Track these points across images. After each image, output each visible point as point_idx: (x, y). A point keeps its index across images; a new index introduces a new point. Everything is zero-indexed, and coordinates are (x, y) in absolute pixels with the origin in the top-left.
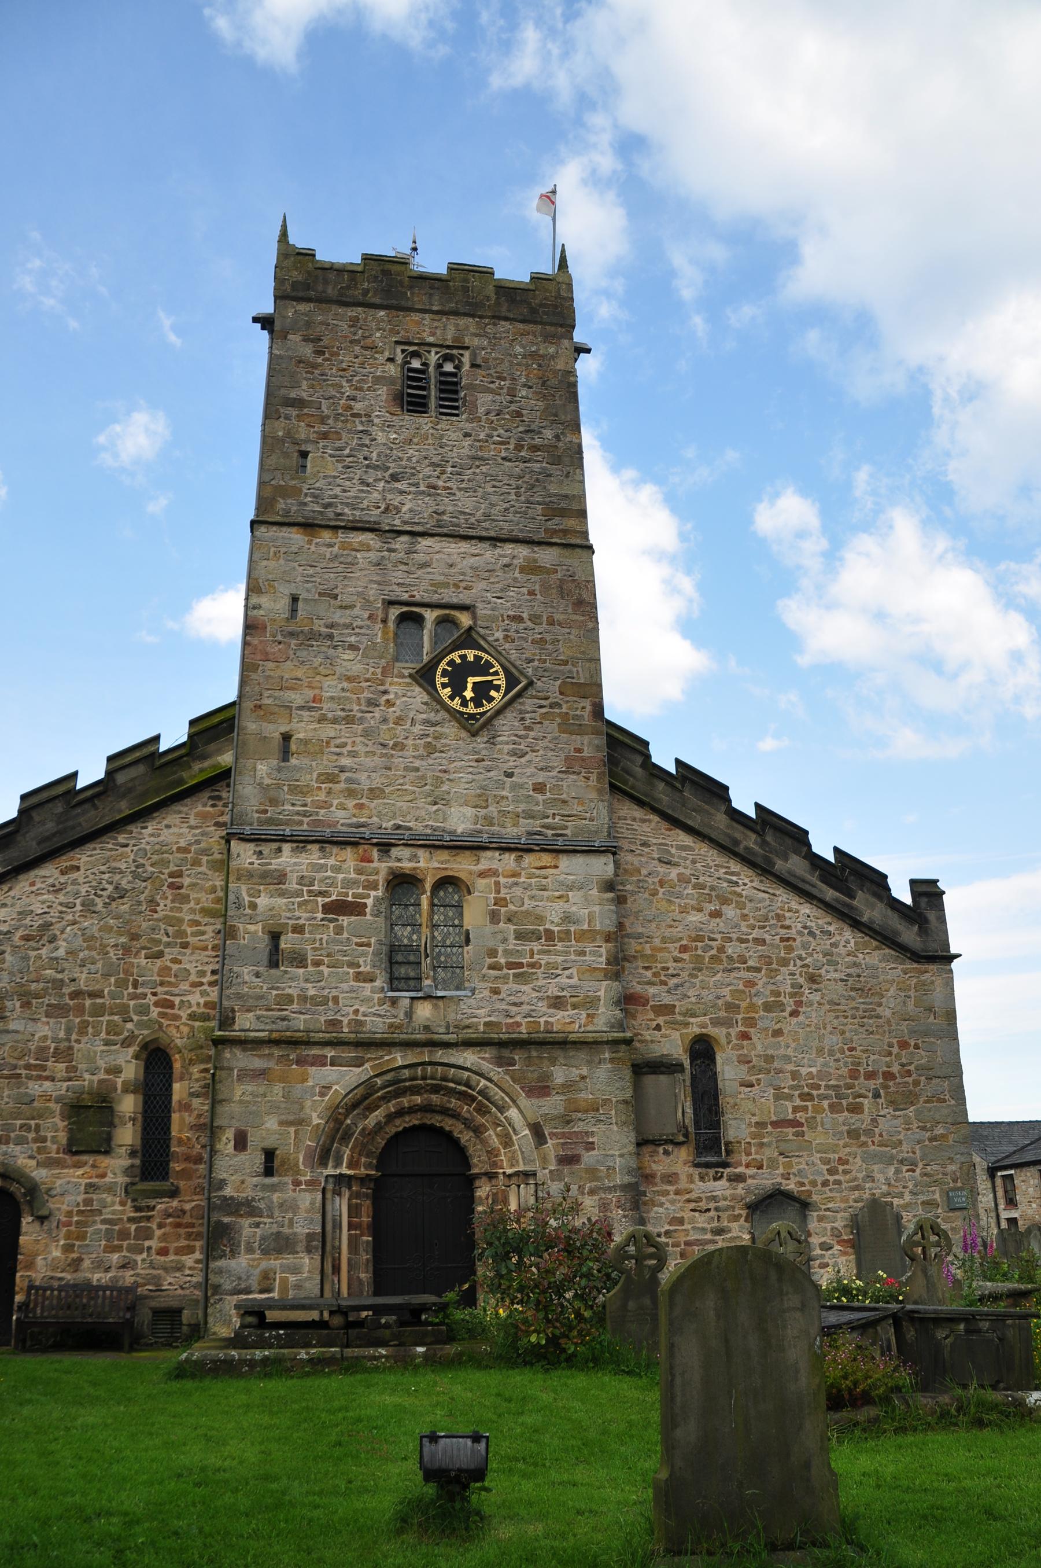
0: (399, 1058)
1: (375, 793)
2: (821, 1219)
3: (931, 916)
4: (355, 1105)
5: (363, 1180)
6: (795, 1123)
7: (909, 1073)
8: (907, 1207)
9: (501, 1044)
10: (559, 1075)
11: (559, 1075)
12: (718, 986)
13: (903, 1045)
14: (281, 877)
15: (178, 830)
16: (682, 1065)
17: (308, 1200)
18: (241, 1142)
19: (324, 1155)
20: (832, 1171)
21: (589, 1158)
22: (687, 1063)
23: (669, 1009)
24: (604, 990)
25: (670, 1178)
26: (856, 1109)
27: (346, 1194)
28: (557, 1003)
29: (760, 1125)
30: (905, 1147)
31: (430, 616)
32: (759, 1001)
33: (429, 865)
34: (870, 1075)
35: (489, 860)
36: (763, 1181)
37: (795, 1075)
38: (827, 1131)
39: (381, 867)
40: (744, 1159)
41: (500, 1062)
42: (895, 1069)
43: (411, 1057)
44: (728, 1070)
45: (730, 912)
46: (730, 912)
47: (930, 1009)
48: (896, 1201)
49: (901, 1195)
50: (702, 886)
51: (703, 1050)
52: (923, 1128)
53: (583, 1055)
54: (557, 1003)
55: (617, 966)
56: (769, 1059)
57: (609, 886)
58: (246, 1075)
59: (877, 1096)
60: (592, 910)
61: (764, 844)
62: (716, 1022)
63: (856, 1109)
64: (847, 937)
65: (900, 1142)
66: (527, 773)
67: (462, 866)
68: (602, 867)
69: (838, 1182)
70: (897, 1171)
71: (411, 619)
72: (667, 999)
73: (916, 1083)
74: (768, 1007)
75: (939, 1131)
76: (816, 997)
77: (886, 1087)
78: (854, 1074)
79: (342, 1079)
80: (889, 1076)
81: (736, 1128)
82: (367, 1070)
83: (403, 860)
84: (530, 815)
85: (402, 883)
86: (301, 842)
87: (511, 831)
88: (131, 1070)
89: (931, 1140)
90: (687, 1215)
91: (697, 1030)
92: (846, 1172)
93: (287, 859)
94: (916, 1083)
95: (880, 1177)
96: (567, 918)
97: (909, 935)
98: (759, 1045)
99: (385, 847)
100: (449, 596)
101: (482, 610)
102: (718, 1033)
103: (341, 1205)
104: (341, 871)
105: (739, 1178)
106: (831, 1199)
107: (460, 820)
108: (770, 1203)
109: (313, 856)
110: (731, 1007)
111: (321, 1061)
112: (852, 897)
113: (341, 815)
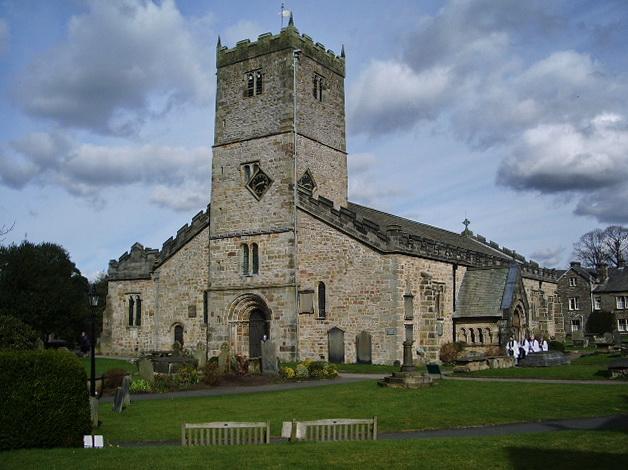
0: (242, 292)
9: (263, 288)
11: (276, 295)
12: (324, 267)
13: (378, 282)
14: (218, 248)
15: (204, 236)
16: (313, 292)
17: (224, 328)
18: (212, 315)
22: (317, 291)
23: (311, 274)
24: (287, 271)
28: (277, 276)
33: (249, 240)
35: (264, 237)
38: (353, 308)
39: (239, 242)
41: (263, 293)
43: (246, 292)
44: (328, 292)
46: (329, 243)
51: (322, 286)
53: (281, 290)
54: (277, 276)
55: (291, 265)
56: (337, 288)
57: (292, 241)
58: (214, 298)
60: (285, 248)
61: (340, 220)
62: (324, 278)
63: (361, 303)
64: (362, 248)
66: (273, 210)
67: (257, 239)
68: (290, 235)
71: (247, 168)
78: (362, 292)
80: (373, 292)
81: (328, 309)
82: (235, 296)
83: (244, 240)
84: (273, 222)
86: (223, 238)
87: (268, 228)
88: (201, 297)
93: (221, 243)
96: (280, 251)
97: (383, 246)
98: (336, 283)
100: (255, 158)
101: (263, 161)
103: (234, 329)
104: (230, 245)
107: (256, 227)
108: (334, 330)
109: (225, 241)
110: (329, 273)
111: (227, 294)
113: (232, 230)
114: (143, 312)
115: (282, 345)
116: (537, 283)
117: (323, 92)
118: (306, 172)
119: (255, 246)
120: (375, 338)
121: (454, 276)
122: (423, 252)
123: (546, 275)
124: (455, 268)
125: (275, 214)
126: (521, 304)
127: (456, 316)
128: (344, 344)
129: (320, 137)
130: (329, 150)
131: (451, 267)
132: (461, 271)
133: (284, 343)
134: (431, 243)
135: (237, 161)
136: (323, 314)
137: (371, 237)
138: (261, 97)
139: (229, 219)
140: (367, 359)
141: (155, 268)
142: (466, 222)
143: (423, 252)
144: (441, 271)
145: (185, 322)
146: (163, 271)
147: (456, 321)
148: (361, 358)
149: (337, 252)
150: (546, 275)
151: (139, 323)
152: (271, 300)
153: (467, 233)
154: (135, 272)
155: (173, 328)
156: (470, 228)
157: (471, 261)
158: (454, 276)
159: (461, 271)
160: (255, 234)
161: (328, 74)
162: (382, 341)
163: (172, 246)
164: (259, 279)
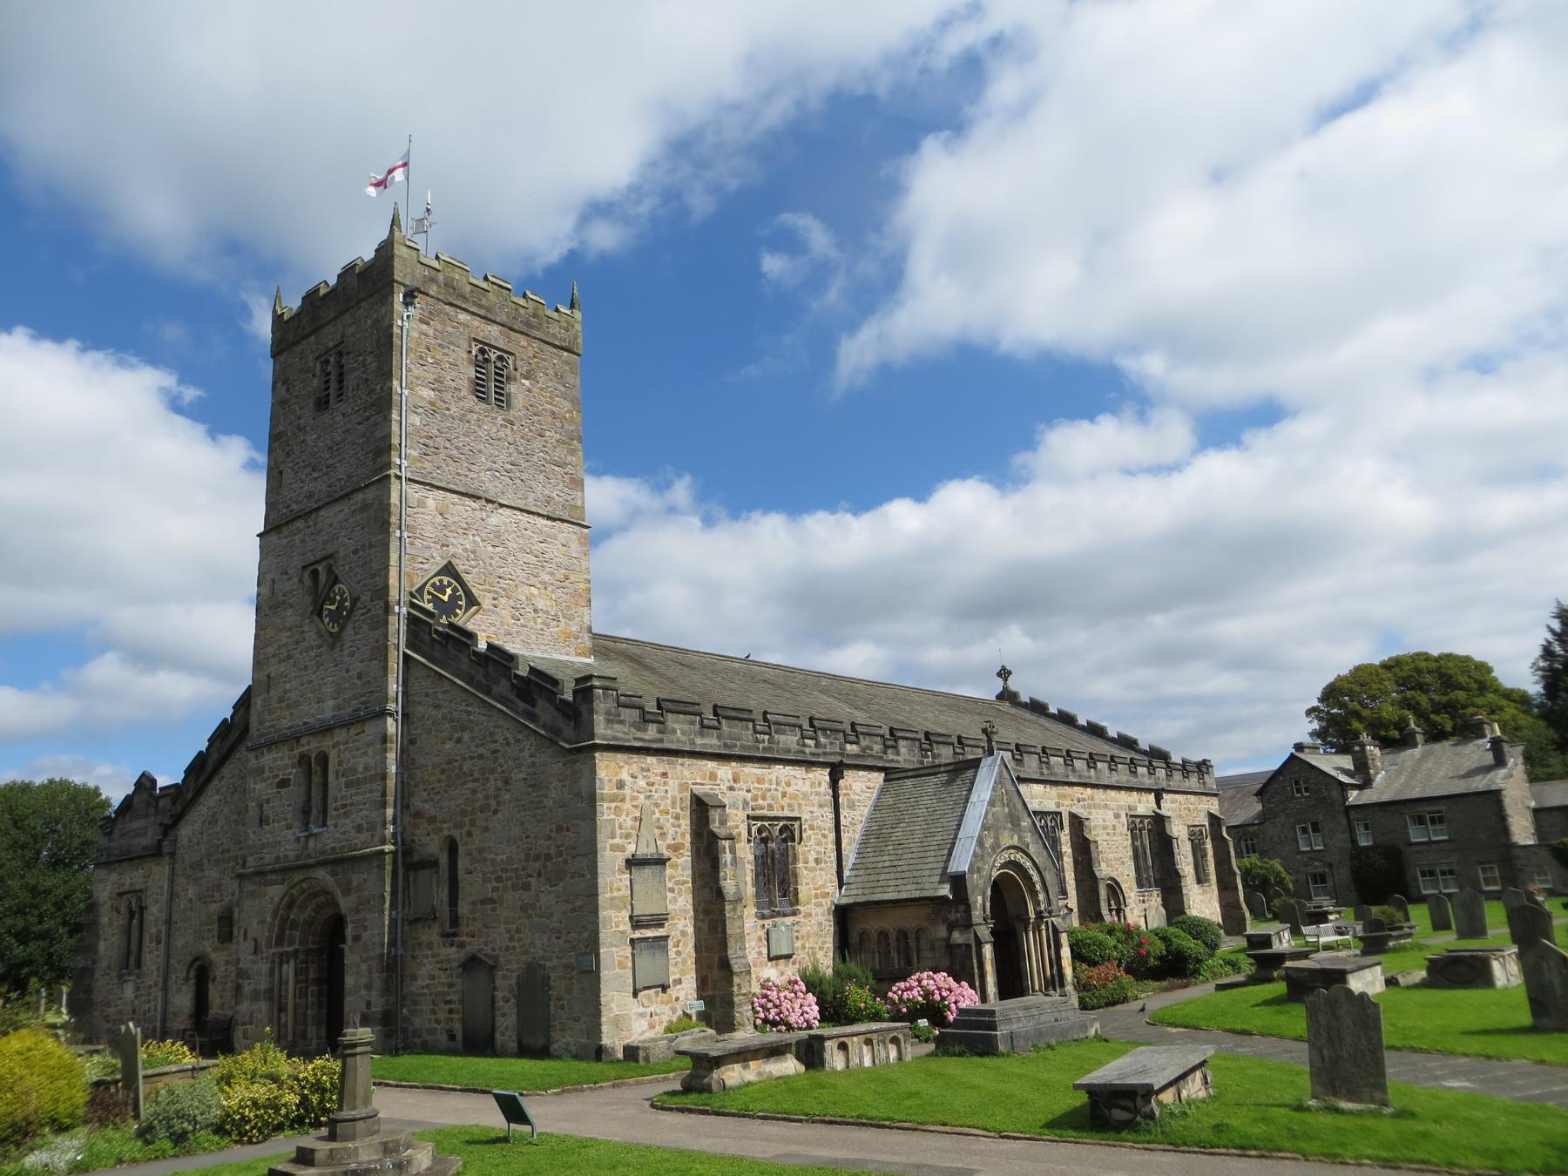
0: (297, 877)
1: (297, 703)
2: (504, 977)
3: (584, 709)
4: (290, 906)
5: (308, 952)
6: (492, 901)
7: (561, 854)
8: (553, 968)
10: (356, 879)
11: (356, 879)
19: (280, 941)
20: (511, 939)
21: (365, 936)
23: (432, 819)
25: (430, 945)
26: (526, 887)
27: (292, 962)
28: (359, 829)
29: (474, 903)
30: (555, 918)
31: (320, 568)
32: (477, 805)
33: (311, 746)
34: (537, 858)
35: (340, 735)
36: (474, 946)
37: (493, 862)
40: (466, 930)
42: (553, 851)
44: (463, 863)
45: (466, 737)
46: (466, 737)
47: (578, 795)
48: (548, 964)
49: (550, 959)
50: (452, 720)
51: (452, 847)
52: (567, 901)
54: (359, 829)
56: (481, 851)
59: (540, 875)
62: (458, 826)
63: (526, 887)
65: (552, 915)
67: (326, 743)
69: (514, 948)
70: (549, 939)
72: (433, 812)
73: (565, 862)
74: (482, 810)
75: (578, 903)
76: (507, 797)
77: (545, 867)
78: (527, 860)
79: (276, 892)
80: (548, 857)
81: (464, 909)
85: (304, 760)
89: (573, 910)
90: (436, 972)
91: (446, 833)
92: (520, 939)
94: (565, 862)
95: (538, 943)
99: (298, 739)
100: (330, 549)
102: (456, 834)
103: (289, 970)
105: (462, 945)
106: (510, 962)
108: (472, 964)
110: (463, 813)
111: (270, 883)
112: (533, 705)
114: (146, 937)
115: (363, 1008)
116: (1152, 797)
117: (512, 388)
118: (449, 569)
119: (323, 759)
120: (558, 986)
121: (836, 797)
122: (701, 743)
123: (1177, 776)
124: (836, 772)
125: (359, 677)
126: (1020, 857)
127: (844, 901)
128: (493, 999)
129: (492, 490)
130: (525, 518)
131: (823, 775)
132: (862, 787)
133: (368, 1004)
134: (740, 715)
135: (297, 562)
136: (455, 920)
137: (544, 710)
138: (343, 407)
139: (281, 700)
140: (540, 1042)
141: (169, 828)
142: (1004, 673)
143: (710, 742)
144: (797, 790)
145: (213, 956)
146: (185, 831)
147: (843, 916)
148: (525, 1042)
149: (481, 757)
150: (1177, 776)
151: (139, 965)
152: (347, 892)
153: (1007, 696)
154: (135, 841)
155: (192, 974)
156: (1013, 684)
157: (905, 755)
158: (836, 797)
159: (862, 787)
160: (326, 730)
161: (523, 347)
162: (569, 990)
163: (202, 770)
164: (330, 838)
